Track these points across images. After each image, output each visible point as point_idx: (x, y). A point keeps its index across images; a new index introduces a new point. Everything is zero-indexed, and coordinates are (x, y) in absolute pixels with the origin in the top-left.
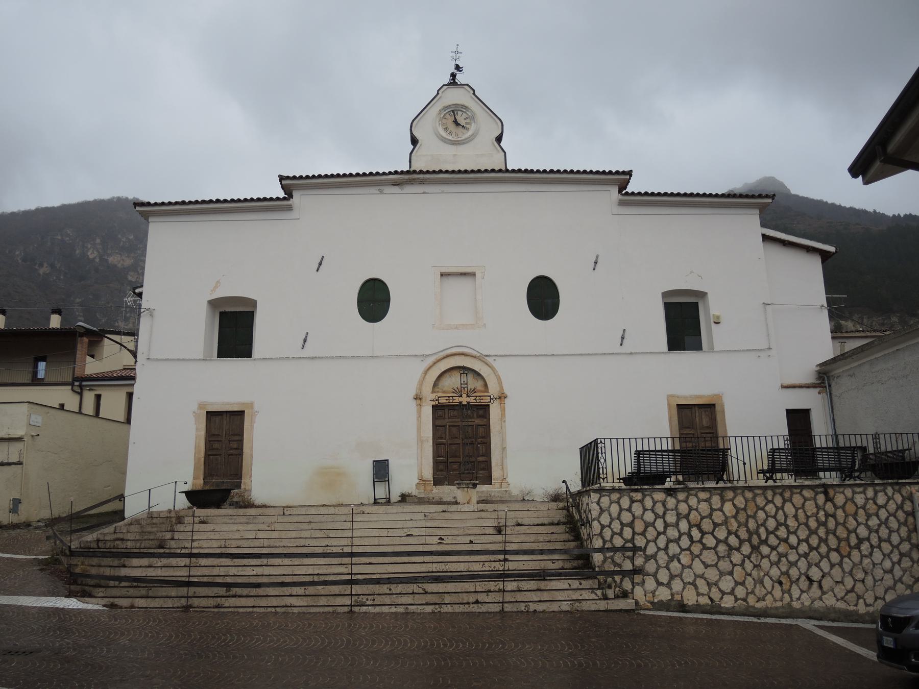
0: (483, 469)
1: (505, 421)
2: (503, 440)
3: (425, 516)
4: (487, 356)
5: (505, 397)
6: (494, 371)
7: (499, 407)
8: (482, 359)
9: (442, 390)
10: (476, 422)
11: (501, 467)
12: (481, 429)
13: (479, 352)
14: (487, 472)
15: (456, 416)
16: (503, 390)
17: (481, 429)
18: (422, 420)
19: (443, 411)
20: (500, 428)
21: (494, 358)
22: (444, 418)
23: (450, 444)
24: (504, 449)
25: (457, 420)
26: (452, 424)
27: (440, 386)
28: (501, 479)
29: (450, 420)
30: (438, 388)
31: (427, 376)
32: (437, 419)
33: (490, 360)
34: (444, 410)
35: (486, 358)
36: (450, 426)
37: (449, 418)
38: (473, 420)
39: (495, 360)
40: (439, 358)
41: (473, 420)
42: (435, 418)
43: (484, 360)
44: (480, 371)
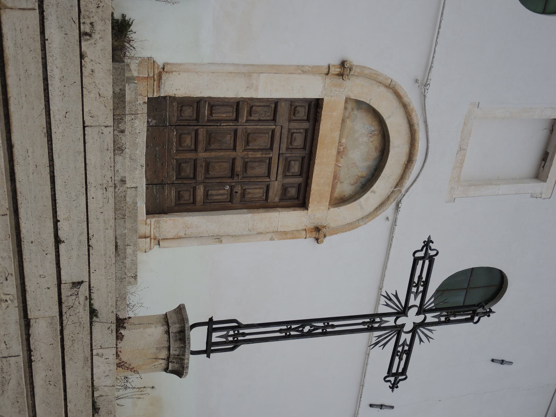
0: (179, 196)
1: (272, 239)
2: (235, 237)
3: (77, 284)
4: (397, 207)
5: (317, 240)
6: (368, 216)
7: (300, 228)
8: (394, 196)
9: (348, 118)
10: (276, 183)
11: (182, 234)
12: (261, 191)
13: (407, 191)
14: (173, 204)
15: (291, 143)
16: (332, 234)
17: (261, 191)
18: (294, 76)
19: (305, 118)
20: (260, 231)
21: (391, 218)
22: (290, 120)
23: (236, 131)
24: (218, 239)
25: (284, 146)
26: (277, 134)
27: (355, 112)
28: (157, 235)
29: (285, 131)
30: (352, 109)
31: (382, 89)
32: (291, 105)
33: (389, 210)
34: (308, 120)
35: (393, 205)
36: (273, 131)
37: (289, 130)
38: (280, 177)
39: (387, 219)
40: (413, 115)
41: (280, 177)
42: (293, 104)
43: (392, 200)
44: (372, 192)
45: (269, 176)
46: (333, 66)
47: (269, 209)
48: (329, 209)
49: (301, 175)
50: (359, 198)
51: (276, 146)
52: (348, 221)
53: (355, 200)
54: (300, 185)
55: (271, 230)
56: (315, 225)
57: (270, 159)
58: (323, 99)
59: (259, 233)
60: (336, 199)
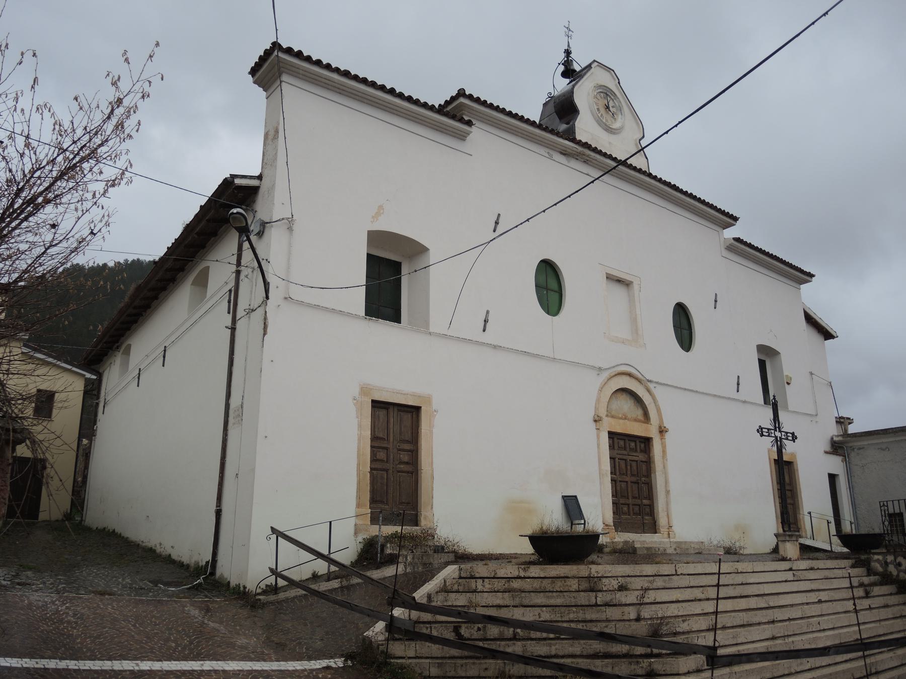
0: (647, 515)
1: (667, 460)
2: (666, 482)
3: (794, 575)
4: (650, 381)
10: (640, 456)
11: (666, 513)
14: (651, 518)
21: (655, 385)
23: (620, 481)
24: (668, 492)
26: (621, 457)
28: (667, 527)
29: (619, 452)
33: (651, 386)
35: (649, 383)
39: (655, 387)
42: (612, 447)
45: (637, 461)
46: (596, 426)
47: (651, 460)
48: (651, 424)
49: (635, 441)
50: (645, 405)
51: (625, 457)
52: (656, 412)
53: (647, 407)
54: (640, 442)
55: (662, 460)
56: (658, 432)
57: (630, 460)
58: (608, 431)
59: (664, 468)
60: (645, 419)
